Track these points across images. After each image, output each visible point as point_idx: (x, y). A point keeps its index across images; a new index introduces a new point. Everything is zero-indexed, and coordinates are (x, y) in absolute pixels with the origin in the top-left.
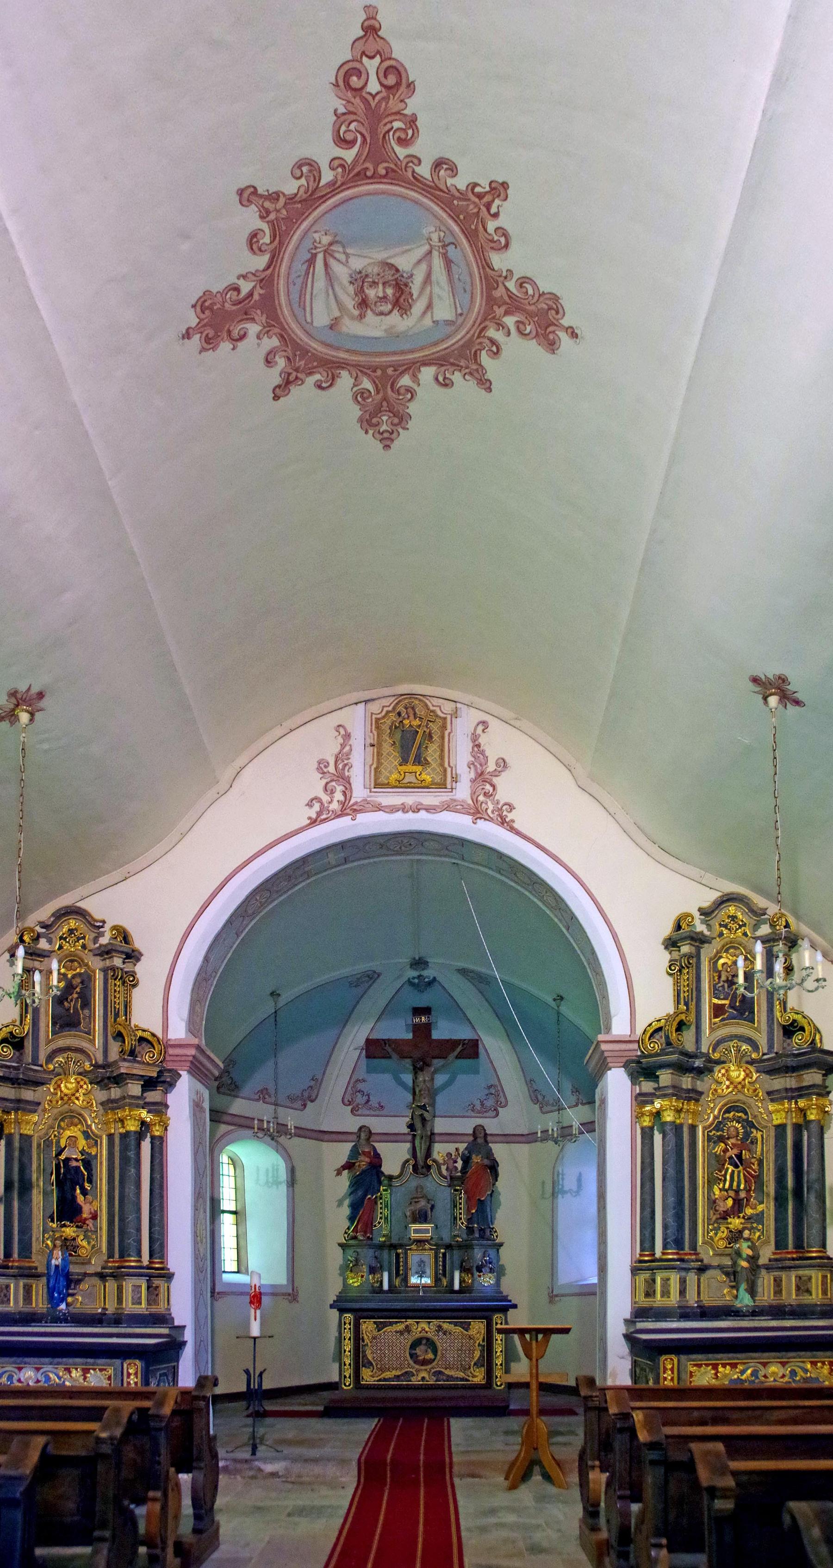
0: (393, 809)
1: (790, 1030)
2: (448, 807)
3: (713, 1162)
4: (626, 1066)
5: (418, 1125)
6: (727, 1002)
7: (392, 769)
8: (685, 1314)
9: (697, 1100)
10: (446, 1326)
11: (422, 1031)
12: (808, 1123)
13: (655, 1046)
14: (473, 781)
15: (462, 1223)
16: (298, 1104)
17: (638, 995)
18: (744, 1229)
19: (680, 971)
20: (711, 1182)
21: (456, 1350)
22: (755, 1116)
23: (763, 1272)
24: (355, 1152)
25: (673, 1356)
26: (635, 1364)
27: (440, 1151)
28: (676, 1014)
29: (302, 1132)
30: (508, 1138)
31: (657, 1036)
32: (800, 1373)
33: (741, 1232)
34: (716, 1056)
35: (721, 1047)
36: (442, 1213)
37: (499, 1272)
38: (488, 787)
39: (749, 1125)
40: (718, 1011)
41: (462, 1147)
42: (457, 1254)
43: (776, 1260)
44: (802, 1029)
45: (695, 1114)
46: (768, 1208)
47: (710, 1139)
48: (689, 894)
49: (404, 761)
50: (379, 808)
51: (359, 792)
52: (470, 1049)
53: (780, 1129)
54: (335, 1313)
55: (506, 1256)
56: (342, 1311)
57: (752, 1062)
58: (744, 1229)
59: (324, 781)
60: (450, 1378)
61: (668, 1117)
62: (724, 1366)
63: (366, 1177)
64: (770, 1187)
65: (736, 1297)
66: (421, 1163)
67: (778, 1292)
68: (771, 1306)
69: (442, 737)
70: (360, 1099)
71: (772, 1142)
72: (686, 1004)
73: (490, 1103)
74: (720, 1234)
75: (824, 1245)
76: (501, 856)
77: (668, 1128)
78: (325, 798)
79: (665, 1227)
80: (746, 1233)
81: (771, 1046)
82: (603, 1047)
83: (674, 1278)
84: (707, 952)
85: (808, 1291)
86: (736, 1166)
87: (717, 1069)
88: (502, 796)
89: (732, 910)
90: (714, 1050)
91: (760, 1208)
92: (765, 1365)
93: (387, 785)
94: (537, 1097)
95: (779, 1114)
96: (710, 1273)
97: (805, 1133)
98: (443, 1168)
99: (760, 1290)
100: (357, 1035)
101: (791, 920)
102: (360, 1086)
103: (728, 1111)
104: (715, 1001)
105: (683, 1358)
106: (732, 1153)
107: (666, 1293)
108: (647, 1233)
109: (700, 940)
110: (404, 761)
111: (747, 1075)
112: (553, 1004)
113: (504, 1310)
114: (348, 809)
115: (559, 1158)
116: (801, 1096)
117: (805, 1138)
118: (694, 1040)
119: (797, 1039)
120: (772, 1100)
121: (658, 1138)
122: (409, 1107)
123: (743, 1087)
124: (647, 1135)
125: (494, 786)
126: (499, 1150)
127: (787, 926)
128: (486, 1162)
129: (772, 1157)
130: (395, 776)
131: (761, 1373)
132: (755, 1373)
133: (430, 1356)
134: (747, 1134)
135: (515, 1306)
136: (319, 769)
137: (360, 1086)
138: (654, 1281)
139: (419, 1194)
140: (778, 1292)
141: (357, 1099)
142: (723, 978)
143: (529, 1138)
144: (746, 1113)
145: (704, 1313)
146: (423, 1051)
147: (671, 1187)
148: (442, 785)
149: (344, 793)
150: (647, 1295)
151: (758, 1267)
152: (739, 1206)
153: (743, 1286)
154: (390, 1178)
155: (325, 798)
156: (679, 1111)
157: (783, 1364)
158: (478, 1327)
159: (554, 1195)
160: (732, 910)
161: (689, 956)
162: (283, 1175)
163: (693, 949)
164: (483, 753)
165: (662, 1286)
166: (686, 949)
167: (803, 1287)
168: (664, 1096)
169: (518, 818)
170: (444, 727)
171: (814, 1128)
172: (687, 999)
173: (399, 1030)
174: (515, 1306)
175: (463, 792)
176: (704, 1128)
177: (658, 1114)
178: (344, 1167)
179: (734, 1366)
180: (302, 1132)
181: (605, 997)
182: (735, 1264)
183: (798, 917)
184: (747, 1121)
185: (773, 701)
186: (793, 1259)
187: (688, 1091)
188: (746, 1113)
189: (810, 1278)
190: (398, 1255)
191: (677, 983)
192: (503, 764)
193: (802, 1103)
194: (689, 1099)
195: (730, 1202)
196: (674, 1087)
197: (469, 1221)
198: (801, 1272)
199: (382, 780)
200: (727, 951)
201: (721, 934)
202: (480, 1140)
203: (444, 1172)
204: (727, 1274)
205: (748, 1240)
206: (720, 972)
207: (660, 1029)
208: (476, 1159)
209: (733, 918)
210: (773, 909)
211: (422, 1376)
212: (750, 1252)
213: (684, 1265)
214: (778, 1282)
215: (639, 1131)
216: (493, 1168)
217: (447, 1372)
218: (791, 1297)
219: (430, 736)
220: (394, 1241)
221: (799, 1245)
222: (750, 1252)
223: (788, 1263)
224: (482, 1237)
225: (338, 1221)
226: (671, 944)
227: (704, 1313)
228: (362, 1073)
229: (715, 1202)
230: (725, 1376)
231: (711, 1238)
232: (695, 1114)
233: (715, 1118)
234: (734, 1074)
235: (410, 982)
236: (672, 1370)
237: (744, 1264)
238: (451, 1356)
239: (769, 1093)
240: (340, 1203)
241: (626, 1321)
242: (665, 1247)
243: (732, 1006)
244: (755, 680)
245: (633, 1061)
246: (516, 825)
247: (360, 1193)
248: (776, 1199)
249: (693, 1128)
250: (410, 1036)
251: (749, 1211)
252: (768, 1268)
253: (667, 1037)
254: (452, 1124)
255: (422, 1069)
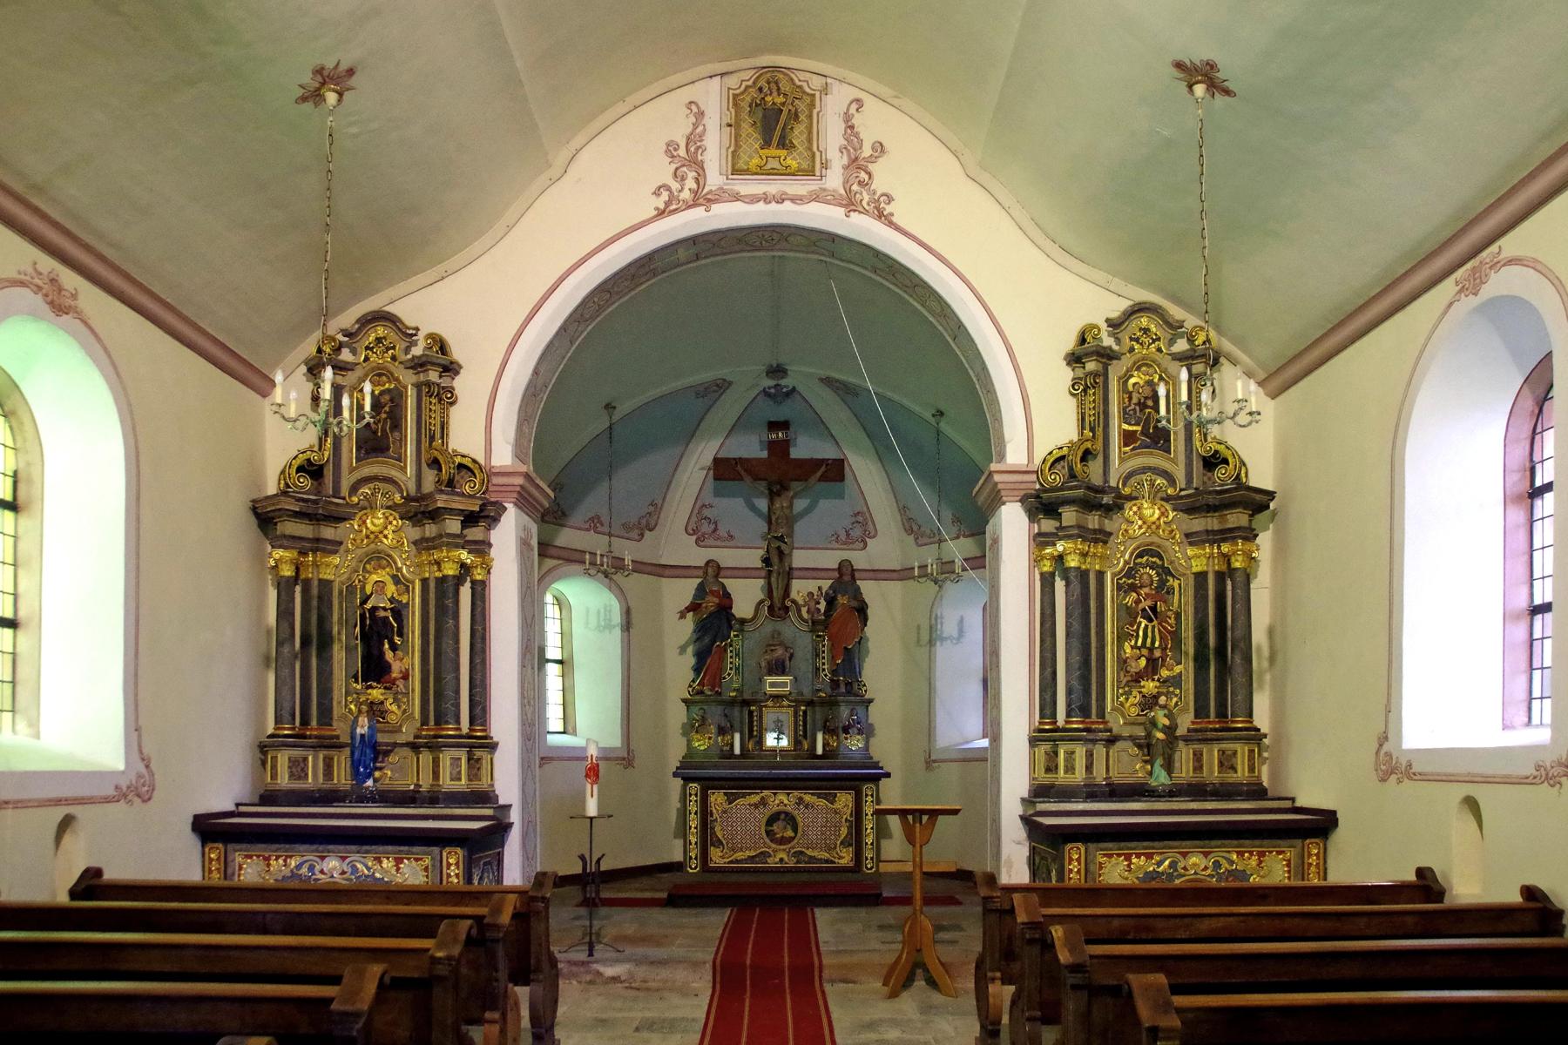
1: (1213, 461)
2: (816, 197)
3: (1124, 613)
4: (1022, 501)
5: (775, 560)
6: (1139, 428)
8: (1092, 793)
9: (1105, 542)
10: (807, 798)
11: (779, 450)
12: (1232, 571)
13: (1055, 479)
14: (846, 168)
15: (825, 675)
16: (634, 534)
17: (1036, 418)
18: (1160, 694)
19: (1085, 391)
20: (1121, 638)
21: (820, 825)
22: (1172, 563)
23: (1181, 744)
24: (701, 591)
25: (1080, 845)
26: (1033, 850)
27: (800, 589)
28: (1082, 441)
29: (641, 567)
30: (878, 574)
31: (1058, 466)
32: (1225, 865)
33: (1156, 697)
34: (1127, 491)
35: (1132, 480)
36: (803, 663)
37: (867, 731)
38: (863, 175)
39: (1165, 572)
40: (1128, 438)
41: (826, 584)
42: (819, 713)
43: (1196, 730)
44: (1225, 461)
45: (1103, 558)
46: (1185, 669)
47: (1119, 587)
48: (1094, 302)
49: (767, 144)
50: (737, 197)
52: (835, 471)
53: (1201, 577)
54: (679, 781)
55: (875, 714)
56: (687, 780)
57: (1167, 499)
58: (1160, 694)
60: (812, 859)
61: (1073, 562)
62: (1138, 856)
63: (714, 622)
64: (1189, 646)
65: (1151, 773)
66: (778, 604)
67: (1198, 767)
68: (1189, 785)
69: (810, 117)
70: (706, 528)
71: (1191, 592)
72: (1092, 429)
73: (857, 532)
74: (1131, 700)
75: (1251, 715)
76: (877, 254)
77: (1072, 575)
79: (1069, 692)
80: (1162, 700)
81: (1189, 480)
82: (997, 478)
83: (1080, 751)
84: (1116, 370)
85: (1234, 769)
86: (1150, 620)
87: (1127, 505)
88: (879, 185)
89: (1144, 322)
90: (1124, 485)
91: (1178, 669)
92: (1184, 855)
94: (913, 527)
95: (1197, 559)
96: (1119, 745)
97: (1229, 582)
98: (804, 610)
99: (1177, 765)
100: (704, 453)
101: (1212, 334)
102: (706, 512)
103: (1140, 556)
104: (1125, 427)
105: (1091, 846)
106: (1146, 604)
107: (1070, 769)
108: (1048, 697)
109: (1107, 356)
110: (767, 144)
111: (1162, 514)
112: (932, 421)
113: (875, 779)
115: (937, 598)
116: (1224, 540)
117: (1229, 587)
118: (1101, 471)
119: (1220, 473)
120: (1191, 544)
121: (1060, 585)
122: (764, 538)
123: (1158, 527)
124: (1047, 582)
125: (870, 175)
126: (868, 588)
127: (1208, 341)
128: (855, 604)
129: (1191, 610)
130: (756, 161)
131: (1180, 865)
132: (1173, 865)
133: (790, 833)
134: (1162, 583)
135: (888, 775)
137: (706, 512)
138: (1056, 754)
139: (775, 641)
140: (1198, 767)
141: (703, 528)
142: (1135, 400)
143: (903, 574)
144: (1161, 558)
145: (1115, 792)
146: (780, 474)
147: (1076, 643)
148: (810, 172)
150: (1048, 770)
151: (1176, 738)
152: (1153, 666)
153: (1159, 762)
154: (743, 621)
156: (1084, 555)
157: (1206, 854)
158: (845, 800)
159: (931, 643)
160: (1144, 322)
161: (1095, 374)
162: (617, 618)
163: (1100, 367)
164: (857, 135)
165: (1066, 760)
166: (1091, 366)
167: (1227, 763)
168: (1069, 537)
169: (896, 210)
170: (812, 105)
171: (1240, 578)
172: (1093, 423)
173: (751, 447)
174: (888, 775)
175: (834, 180)
176: (1114, 575)
177: (1060, 558)
178: (688, 609)
179: (1149, 856)
180: (641, 567)
181: (998, 419)
182: (1149, 735)
183: (1218, 328)
184: (1163, 566)
185: (1200, 90)
186: (1216, 730)
187: (1095, 531)
188: (1161, 558)
189: (1235, 753)
190: (751, 713)
191: (1081, 405)
192: (879, 148)
193: (1225, 548)
194: (1096, 541)
195: (1143, 662)
196: (1079, 527)
197: (834, 672)
198: (1224, 746)
199: (741, 165)
200: (1138, 369)
201: (1132, 350)
202: (846, 577)
203: (805, 616)
204: (1140, 746)
205: (1164, 707)
206: (1130, 393)
207: (1062, 458)
208: (842, 600)
209: (1146, 331)
210: (1191, 321)
211: (780, 857)
212: (1167, 722)
213: (1091, 736)
214: (1198, 757)
215: (1038, 577)
216: (862, 611)
217: (809, 852)
218: (1212, 773)
219: (796, 116)
220: (747, 696)
221: (1222, 714)
222: (1167, 722)
223: (1210, 735)
224: (849, 693)
225: (680, 671)
226: (1074, 359)
227: (1115, 792)
228: (708, 498)
229: (1125, 661)
230: (1140, 868)
231: (1122, 704)
232: (1103, 558)
233: (1126, 563)
234: (1147, 512)
235: (765, 393)
236: (1078, 860)
237: (1160, 735)
238: (813, 835)
239: (1187, 535)
240: (683, 650)
241: (1023, 800)
242: (1069, 715)
243: (1145, 432)
244: (1179, 65)
245: (1031, 496)
246: (894, 219)
247: (707, 640)
248: (1196, 659)
249: (1100, 575)
250: (765, 454)
251: (1165, 673)
252: (1187, 740)
253: (1071, 469)
254: (814, 557)
255: (779, 494)
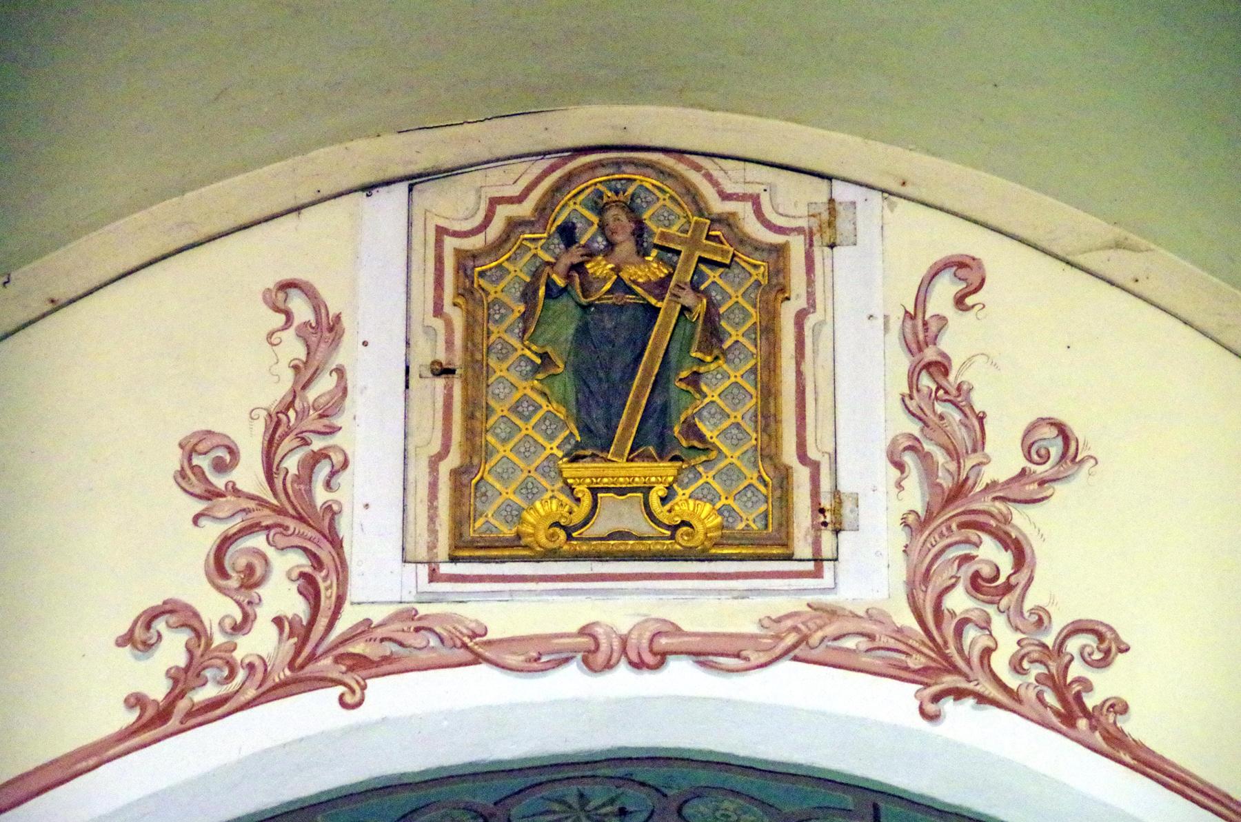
0: (540, 656)
2: (797, 643)
7: (535, 472)
14: (916, 525)
38: (991, 553)
49: (594, 439)
50: (472, 649)
51: (380, 578)
59: (212, 532)
78: (215, 608)
93: (514, 547)
110: (594, 439)
114: (327, 656)
125: (1020, 552)
130: (550, 506)
136: (187, 475)
148: (771, 544)
149: (309, 587)
155: (215, 608)
199: (489, 521)
